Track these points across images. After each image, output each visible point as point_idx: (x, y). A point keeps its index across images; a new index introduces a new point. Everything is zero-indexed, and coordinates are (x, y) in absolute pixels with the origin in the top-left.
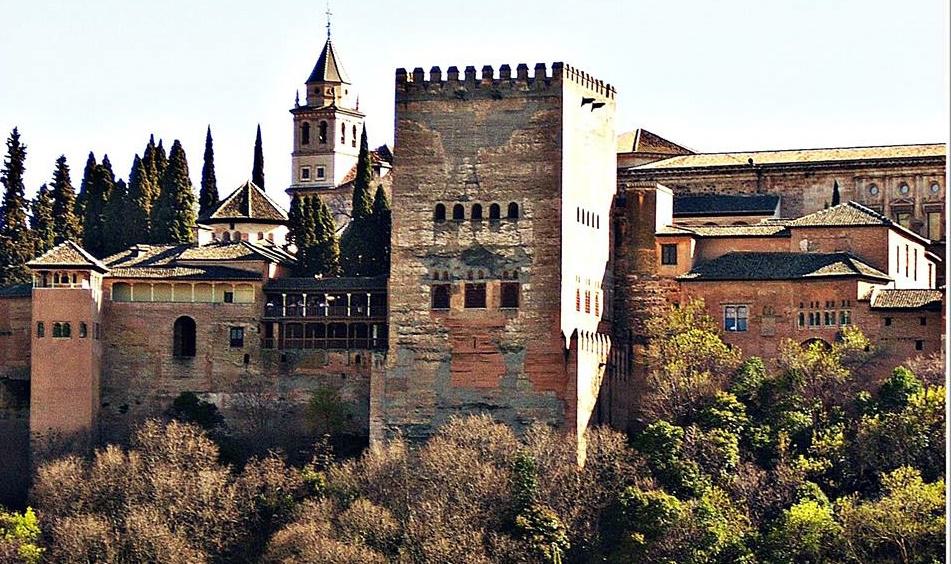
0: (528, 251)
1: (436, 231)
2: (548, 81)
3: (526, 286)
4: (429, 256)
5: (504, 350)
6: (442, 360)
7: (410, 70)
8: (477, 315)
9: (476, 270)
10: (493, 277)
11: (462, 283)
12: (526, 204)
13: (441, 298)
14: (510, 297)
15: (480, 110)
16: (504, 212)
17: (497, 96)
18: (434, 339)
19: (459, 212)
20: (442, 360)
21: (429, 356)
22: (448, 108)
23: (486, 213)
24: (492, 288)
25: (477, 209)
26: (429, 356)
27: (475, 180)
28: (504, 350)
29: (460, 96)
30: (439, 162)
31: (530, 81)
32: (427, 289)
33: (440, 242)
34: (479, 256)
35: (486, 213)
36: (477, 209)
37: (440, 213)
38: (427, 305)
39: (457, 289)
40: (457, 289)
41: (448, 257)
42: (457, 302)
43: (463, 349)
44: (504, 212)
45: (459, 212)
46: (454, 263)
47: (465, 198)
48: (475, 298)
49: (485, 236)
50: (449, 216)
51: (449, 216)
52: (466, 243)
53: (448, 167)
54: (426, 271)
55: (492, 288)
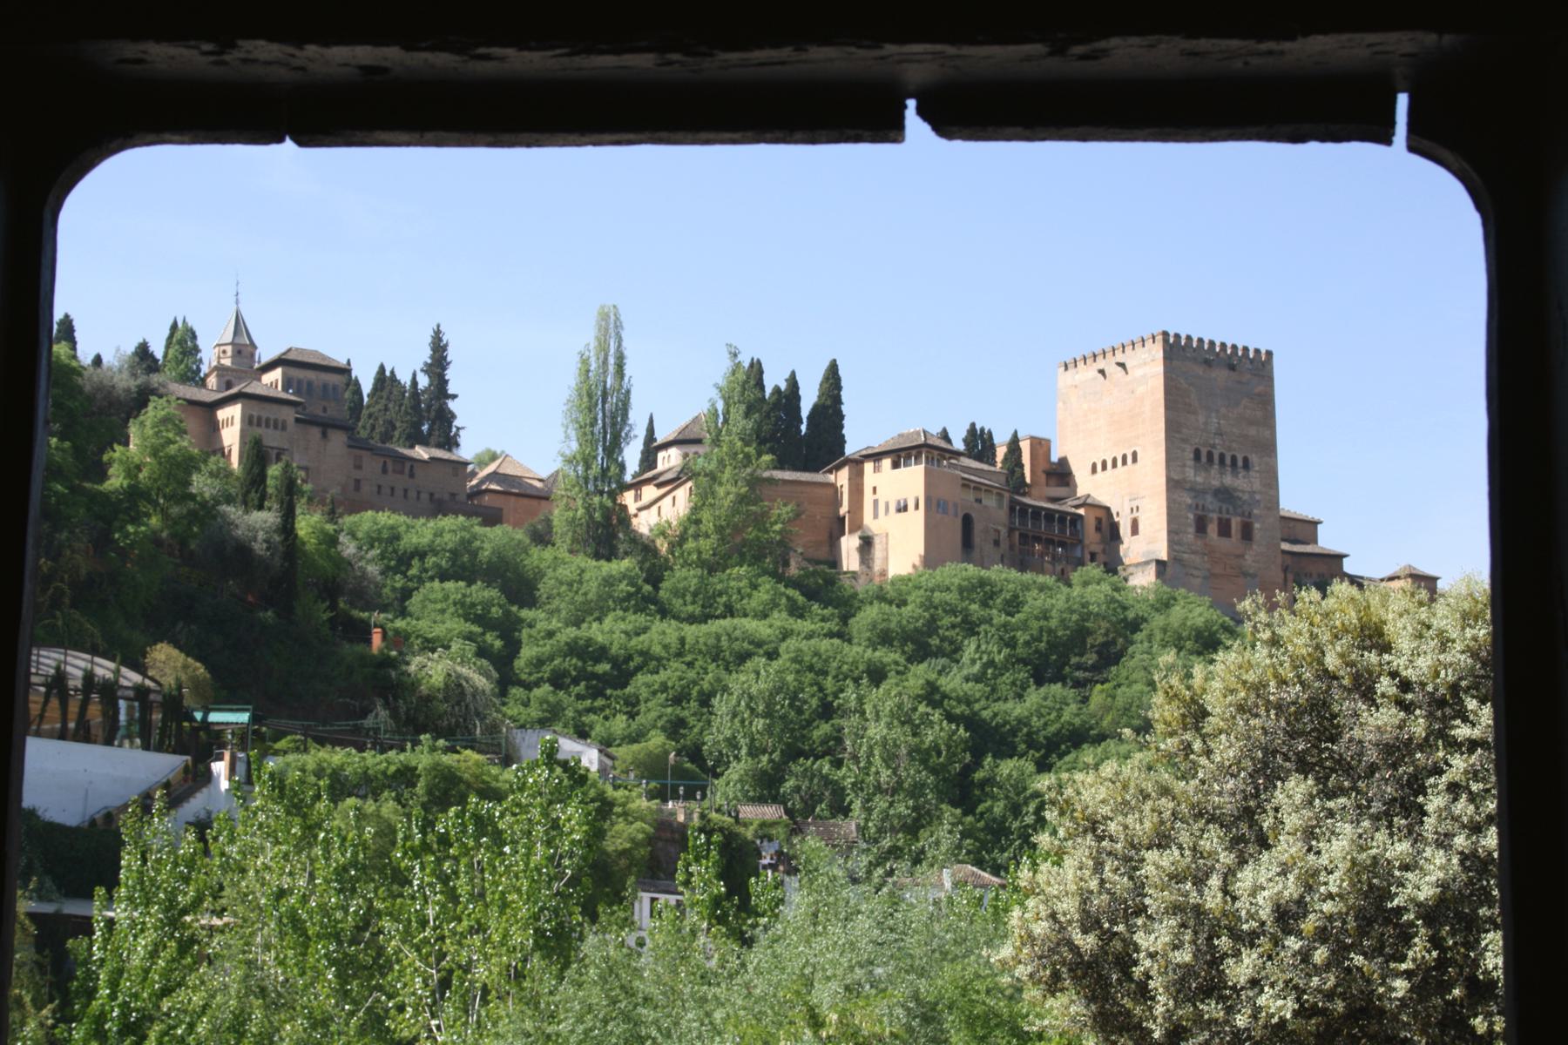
0: (1258, 497)
1: (1196, 470)
2: (1263, 364)
3: (1257, 526)
4: (1191, 489)
5: (1245, 574)
6: (1205, 578)
7: (1172, 334)
8: (1224, 542)
9: (1224, 507)
10: (1237, 514)
11: (1215, 516)
12: (1254, 458)
13: (1201, 526)
14: (1247, 533)
15: (1221, 375)
16: (1240, 463)
17: (1232, 368)
18: (1197, 559)
19: (1210, 455)
20: (1205, 578)
21: (1196, 572)
22: (1199, 370)
23: (1228, 461)
24: (1235, 523)
25: (1222, 457)
26: (1196, 572)
27: (1220, 433)
28: (1245, 574)
29: (1207, 363)
30: (1195, 413)
31: (1252, 361)
32: (1191, 516)
33: (1199, 479)
34: (1225, 494)
35: (1228, 461)
36: (1222, 457)
37: (1197, 454)
38: (1192, 530)
39: (1211, 520)
40: (1211, 520)
41: (1204, 492)
42: (1212, 529)
43: (1218, 570)
44: (1240, 463)
45: (1210, 455)
46: (1209, 498)
47: (1214, 446)
48: (1224, 530)
49: (1228, 480)
50: (1204, 459)
51: (1204, 459)
52: (1216, 483)
53: (1201, 419)
54: (1189, 501)
55: (1235, 523)
